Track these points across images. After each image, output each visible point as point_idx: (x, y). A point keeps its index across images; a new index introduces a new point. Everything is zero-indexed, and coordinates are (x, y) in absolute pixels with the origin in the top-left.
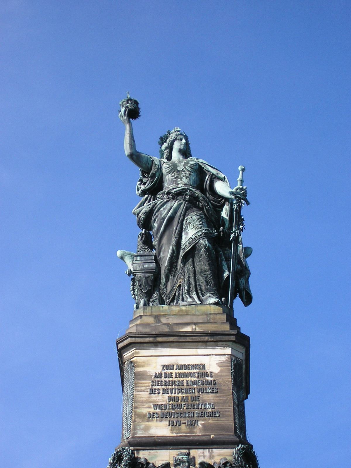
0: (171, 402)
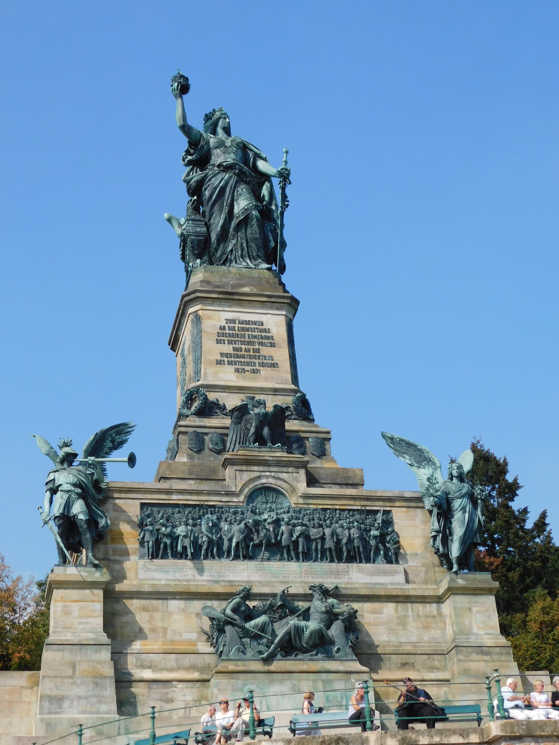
0: (235, 352)
